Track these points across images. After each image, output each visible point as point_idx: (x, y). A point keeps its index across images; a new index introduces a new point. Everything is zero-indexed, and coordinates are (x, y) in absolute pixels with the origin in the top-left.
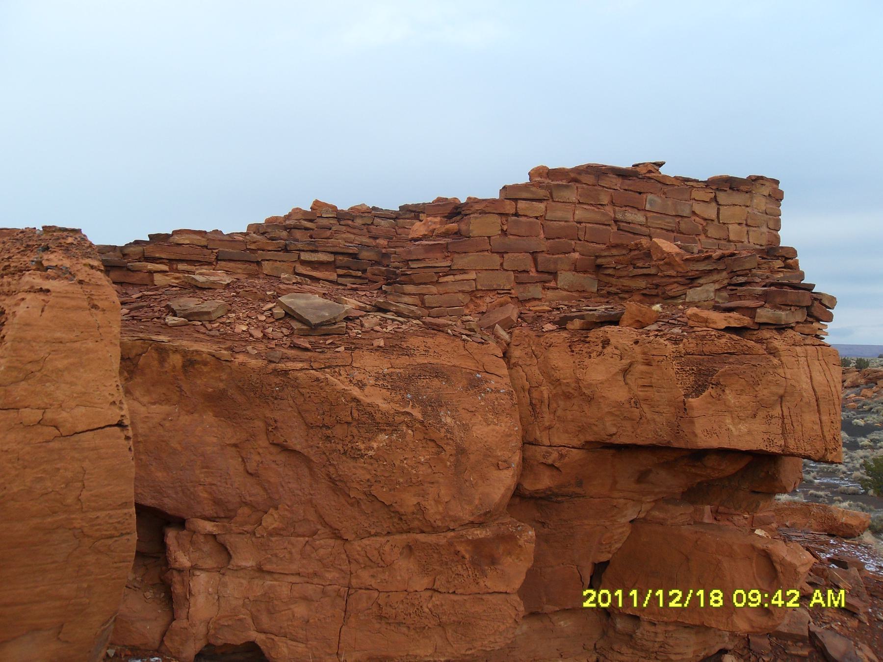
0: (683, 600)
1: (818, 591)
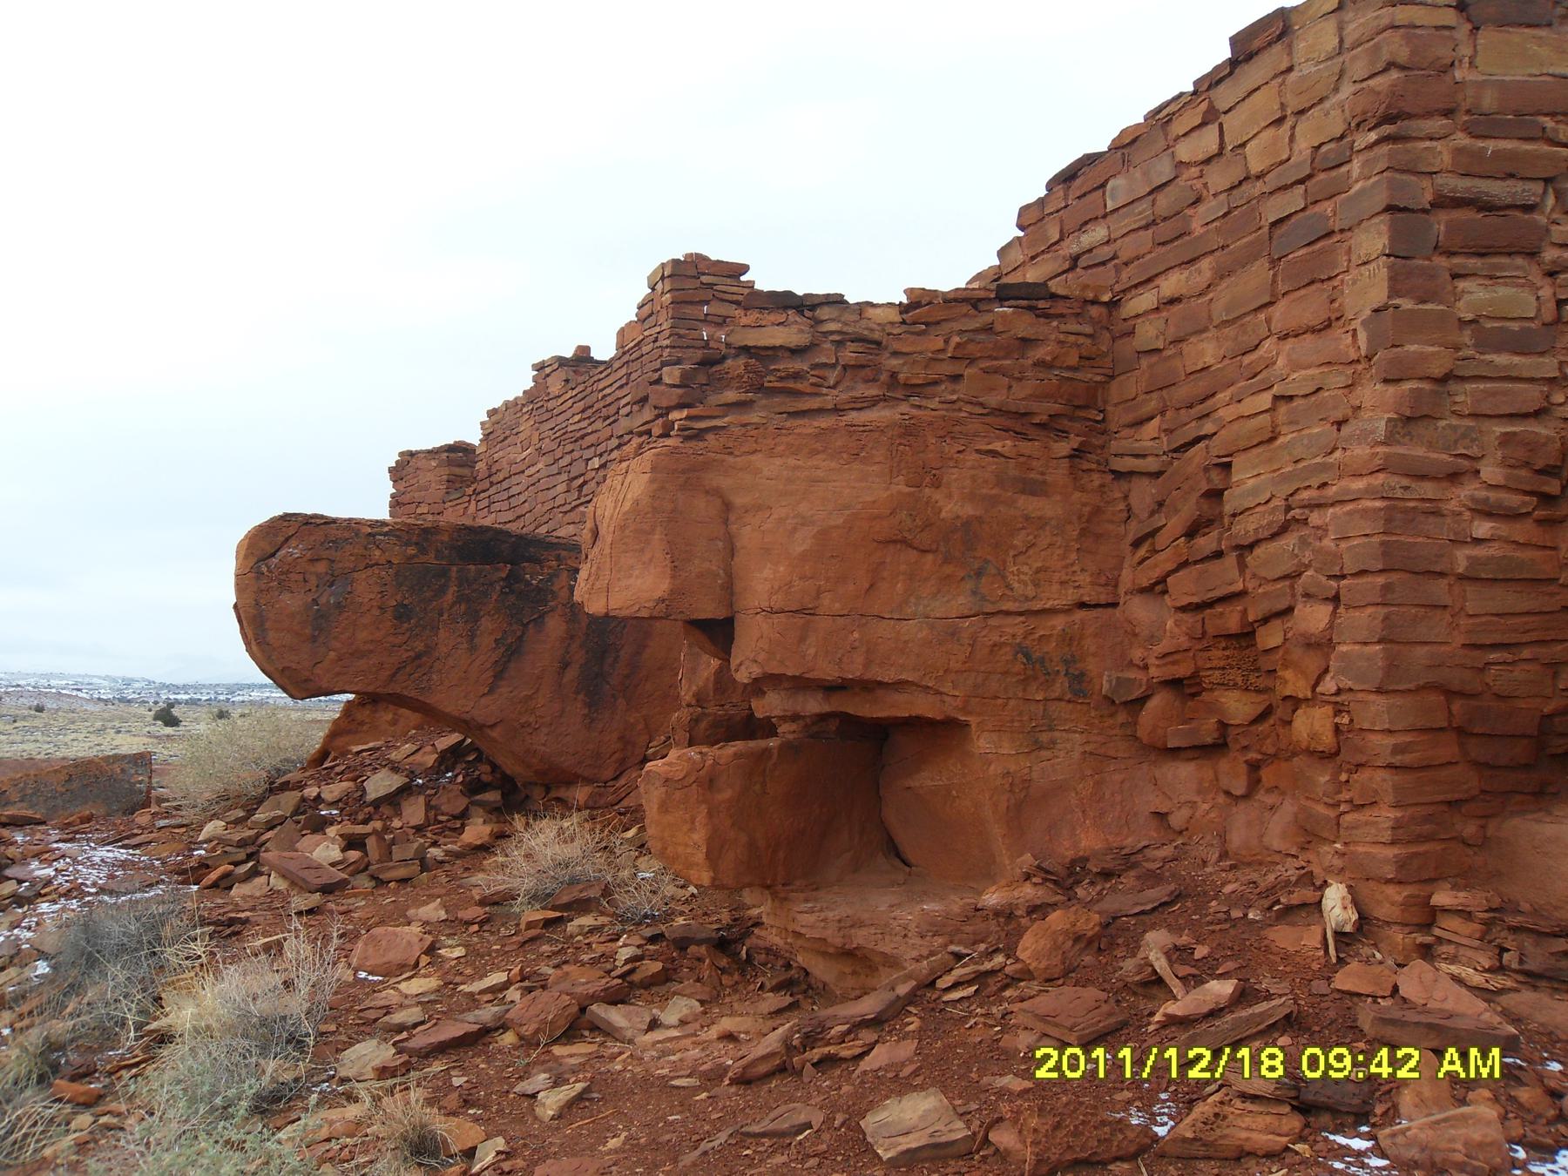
0: (1211, 1068)
1: (1452, 1050)
